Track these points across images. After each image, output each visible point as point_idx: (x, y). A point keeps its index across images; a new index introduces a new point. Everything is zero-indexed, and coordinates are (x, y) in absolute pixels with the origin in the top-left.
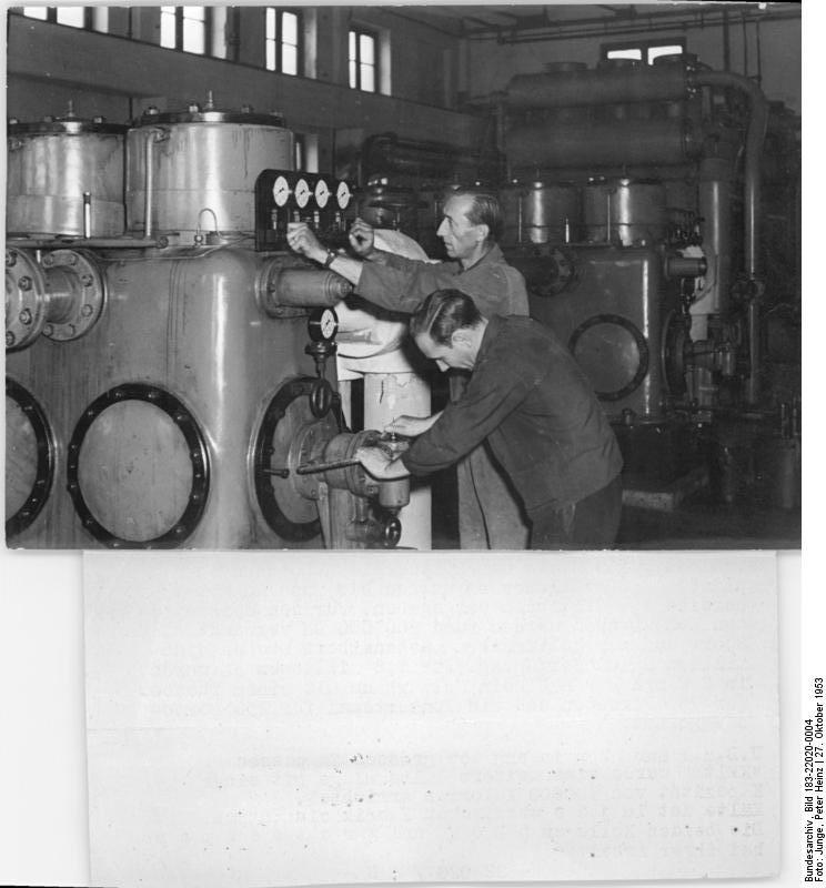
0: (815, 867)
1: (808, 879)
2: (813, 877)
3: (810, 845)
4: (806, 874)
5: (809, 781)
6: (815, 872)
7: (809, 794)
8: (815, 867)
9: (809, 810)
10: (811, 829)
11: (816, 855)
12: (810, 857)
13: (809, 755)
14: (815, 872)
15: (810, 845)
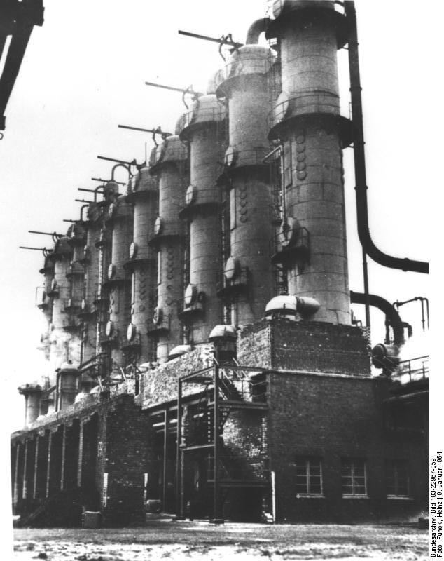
0: (437, 548)
1: (433, 556)
2: (436, 554)
3: (434, 534)
4: (430, 552)
5: (433, 493)
6: (437, 551)
7: (433, 502)
8: (437, 548)
9: (433, 512)
10: (434, 523)
11: (437, 541)
12: (434, 541)
13: (433, 484)
14: (437, 551)
15: (434, 534)
